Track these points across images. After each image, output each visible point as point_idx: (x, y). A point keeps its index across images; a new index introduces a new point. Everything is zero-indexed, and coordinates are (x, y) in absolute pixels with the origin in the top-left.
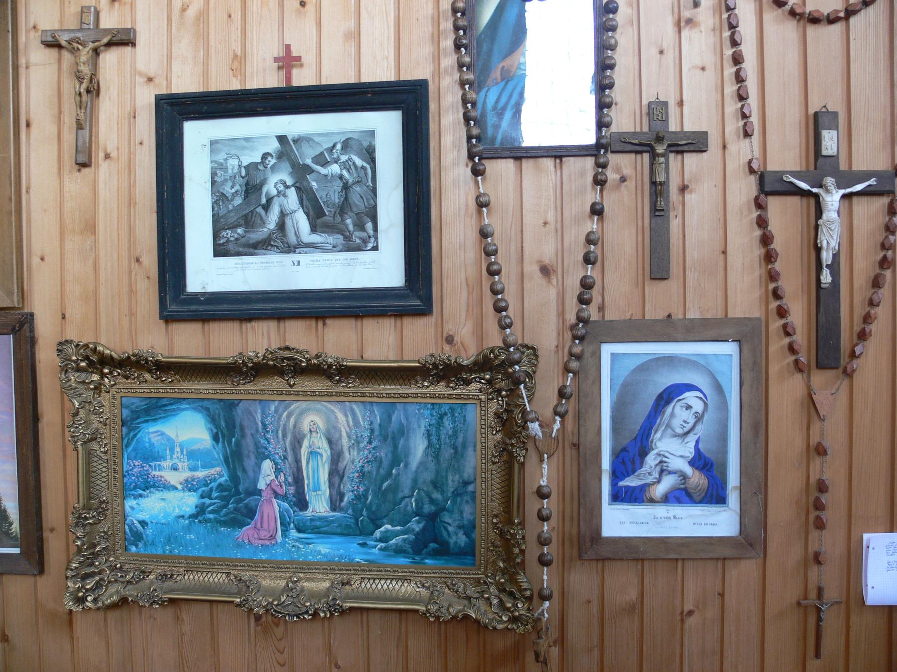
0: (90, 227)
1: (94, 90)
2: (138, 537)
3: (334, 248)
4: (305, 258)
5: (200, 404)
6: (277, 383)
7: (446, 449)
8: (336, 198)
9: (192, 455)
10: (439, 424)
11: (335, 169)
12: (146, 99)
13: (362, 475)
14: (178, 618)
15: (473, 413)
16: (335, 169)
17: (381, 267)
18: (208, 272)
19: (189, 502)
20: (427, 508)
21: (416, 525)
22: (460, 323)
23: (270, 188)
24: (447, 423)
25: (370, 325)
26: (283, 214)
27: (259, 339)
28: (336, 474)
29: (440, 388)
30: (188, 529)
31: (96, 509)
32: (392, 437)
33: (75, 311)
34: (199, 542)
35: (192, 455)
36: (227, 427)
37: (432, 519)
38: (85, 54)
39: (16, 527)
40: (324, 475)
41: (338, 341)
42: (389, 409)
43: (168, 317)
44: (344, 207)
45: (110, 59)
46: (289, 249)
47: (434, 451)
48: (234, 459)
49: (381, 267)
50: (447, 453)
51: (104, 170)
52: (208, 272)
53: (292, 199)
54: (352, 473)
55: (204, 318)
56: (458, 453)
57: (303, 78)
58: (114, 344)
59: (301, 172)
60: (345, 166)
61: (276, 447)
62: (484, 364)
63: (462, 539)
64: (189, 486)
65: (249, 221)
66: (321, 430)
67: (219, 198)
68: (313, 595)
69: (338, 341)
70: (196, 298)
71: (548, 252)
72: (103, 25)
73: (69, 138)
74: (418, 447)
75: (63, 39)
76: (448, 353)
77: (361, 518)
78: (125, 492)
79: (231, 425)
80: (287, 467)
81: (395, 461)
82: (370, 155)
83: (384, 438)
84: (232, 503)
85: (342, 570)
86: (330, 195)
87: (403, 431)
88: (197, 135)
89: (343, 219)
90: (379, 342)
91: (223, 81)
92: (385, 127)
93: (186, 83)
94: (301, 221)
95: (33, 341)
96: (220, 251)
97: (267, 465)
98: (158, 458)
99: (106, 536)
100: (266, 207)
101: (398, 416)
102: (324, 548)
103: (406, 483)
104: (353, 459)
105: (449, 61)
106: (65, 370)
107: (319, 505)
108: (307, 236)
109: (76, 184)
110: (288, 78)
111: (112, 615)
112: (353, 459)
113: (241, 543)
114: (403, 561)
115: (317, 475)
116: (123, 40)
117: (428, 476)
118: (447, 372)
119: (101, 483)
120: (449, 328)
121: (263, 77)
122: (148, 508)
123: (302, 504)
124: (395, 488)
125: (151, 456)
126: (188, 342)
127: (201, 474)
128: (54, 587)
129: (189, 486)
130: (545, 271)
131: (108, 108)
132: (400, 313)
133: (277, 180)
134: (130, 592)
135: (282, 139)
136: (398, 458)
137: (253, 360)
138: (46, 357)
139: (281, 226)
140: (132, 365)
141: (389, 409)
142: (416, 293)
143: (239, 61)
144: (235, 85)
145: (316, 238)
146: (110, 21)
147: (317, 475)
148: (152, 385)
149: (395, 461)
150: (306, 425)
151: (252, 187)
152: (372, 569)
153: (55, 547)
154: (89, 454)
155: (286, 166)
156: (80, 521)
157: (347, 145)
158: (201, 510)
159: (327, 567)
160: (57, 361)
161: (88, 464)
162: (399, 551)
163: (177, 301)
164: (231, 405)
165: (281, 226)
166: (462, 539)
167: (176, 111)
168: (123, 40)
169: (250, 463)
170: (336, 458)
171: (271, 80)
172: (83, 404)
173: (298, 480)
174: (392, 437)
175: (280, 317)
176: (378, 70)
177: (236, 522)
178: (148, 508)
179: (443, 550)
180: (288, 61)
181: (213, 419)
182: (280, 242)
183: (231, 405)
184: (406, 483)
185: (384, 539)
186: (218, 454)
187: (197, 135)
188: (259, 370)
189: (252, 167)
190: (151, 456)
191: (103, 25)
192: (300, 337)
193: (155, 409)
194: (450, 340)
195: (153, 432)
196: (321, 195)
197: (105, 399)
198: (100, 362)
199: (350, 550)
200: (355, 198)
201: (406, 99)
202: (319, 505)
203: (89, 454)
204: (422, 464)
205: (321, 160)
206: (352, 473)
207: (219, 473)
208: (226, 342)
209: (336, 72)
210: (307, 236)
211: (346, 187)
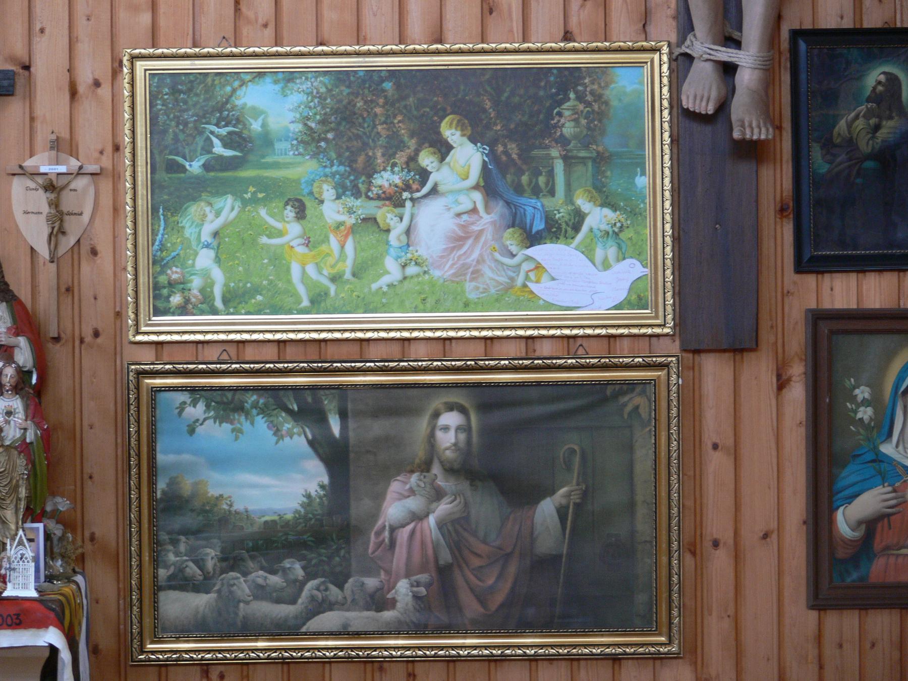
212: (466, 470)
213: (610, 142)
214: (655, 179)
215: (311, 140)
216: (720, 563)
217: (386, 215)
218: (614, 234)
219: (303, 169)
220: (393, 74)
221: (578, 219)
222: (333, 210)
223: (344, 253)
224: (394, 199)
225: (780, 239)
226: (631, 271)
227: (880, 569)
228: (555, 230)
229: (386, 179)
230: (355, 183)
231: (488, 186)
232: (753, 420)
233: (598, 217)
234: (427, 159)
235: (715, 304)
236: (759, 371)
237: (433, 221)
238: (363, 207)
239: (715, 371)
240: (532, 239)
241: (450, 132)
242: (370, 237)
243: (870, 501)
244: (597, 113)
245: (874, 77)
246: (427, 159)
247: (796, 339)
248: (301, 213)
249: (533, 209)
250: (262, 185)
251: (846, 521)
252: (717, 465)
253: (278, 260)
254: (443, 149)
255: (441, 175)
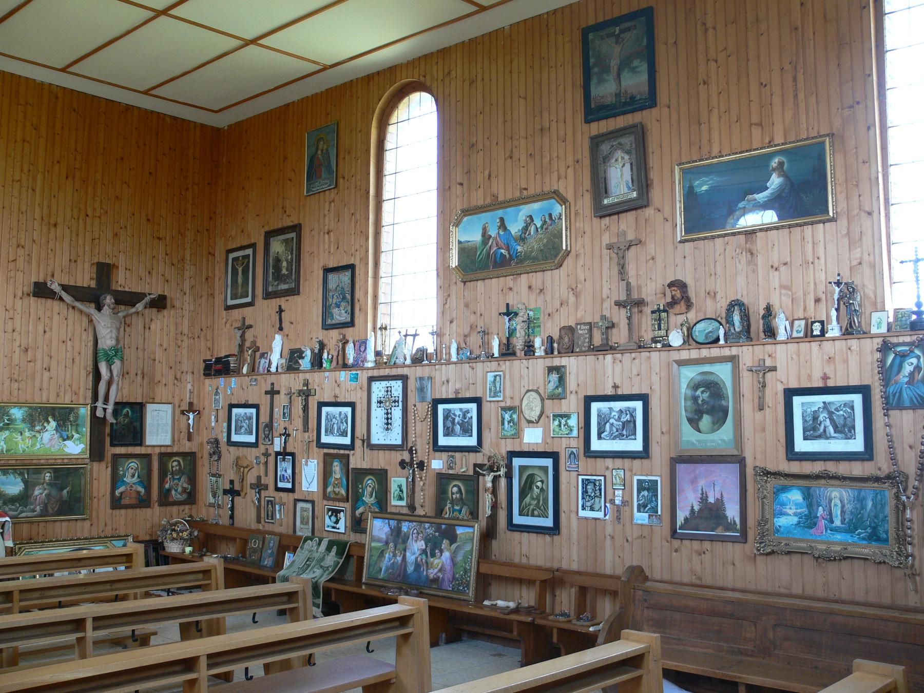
0: (763, 430)
1: (764, 386)
2: (778, 531)
3: (842, 438)
4: (832, 441)
5: (798, 487)
6: (823, 481)
7: (879, 505)
8: (842, 422)
9: (796, 504)
10: (876, 497)
11: (841, 412)
12: (780, 388)
13: (852, 513)
14: (791, 560)
15: (887, 493)
16: (841, 412)
17: (857, 445)
18: (801, 445)
19: (795, 520)
20: (873, 525)
21: (869, 530)
22: (881, 464)
23: (821, 418)
24: (879, 497)
25: (853, 464)
26: (825, 427)
27: (817, 467)
28: (843, 512)
29: (876, 485)
30: (795, 529)
31: (763, 521)
32: (861, 500)
33: (759, 457)
34: (798, 533)
35: (796, 504)
36: (808, 495)
37: (874, 529)
38: (761, 375)
39: (738, 527)
40: (839, 513)
41: (843, 468)
42: (860, 491)
43: (789, 459)
44: (844, 425)
45: (769, 375)
46: (827, 438)
47: (875, 505)
48: (810, 506)
49: (857, 445)
50: (879, 506)
51: (767, 410)
52: (801, 445)
53: (828, 422)
54: (848, 512)
55: (801, 460)
56: (883, 506)
57: (831, 383)
58: (771, 467)
59: (831, 414)
60: (845, 412)
61: (823, 503)
62: (888, 477)
63: (885, 536)
64: (795, 514)
65: (814, 429)
66: (838, 498)
67: (805, 421)
68: (835, 552)
69: (843, 468)
70: (797, 453)
71: (911, 440)
72: (767, 365)
73: (756, 401)
74: (870, 504)
75: (754, 369)
76: (879, 473)
77: (851, 527)
78: (774, 516)
79: (809, 494)
80: (827, 509)
81: (862, 508)
82: (852, 408)
83: (858, 500)
84: (809, 521)
85: (845, 545)
86: (840, 422)
87: (864, 499)
88: (797, 401)
89: (845, 430)
90: (857, 469)
91: (806, 384)
92: (857, 399)
93: (794, 385)
94: (831, 429)
95: (745, 466)
96: (805, 438)
97: (820, 508)
98: (785, 505)
99: (768, 530)
100: (820, 425)
101: (863, 493)
102: (839, 537)
103: (866, 515)
104: (849, 507)
105: (877, 377)
106: (756, 475)
107: (838, 522)
108: (833, 434)
109: (759, 415)
110: (826, 383)
111: (769, 557)
112: (849, 507)
113: (811, 534)
114: (865, 542)
115: (837, 512)
116: (774, 369)
117: (873, 514)
118: (877, 479)
119: (766, 512)
120: (879, 465)
121: (817, 383)
122: (781, 522)
123: (832, 522)
124: (862, 517)
125: (783, 504)
126: (795, 467)
127: (799, 511)
128: (750, 547)
129: (795, 514)
130: (911, 447)
131: (768, 391)
132: (863, 460)
133: (823, 416)
134: (775, 549)
135: (824, 403)
136: (863, 507)
137: (815, 474)
138: (749, 471)
139: (825, 431)
140: (777, 474)
141: (860, 491)
142: (868, 454)
143: (809, 377)
144: (809, 386)
145: (836, 435)
146: (768, 363)
147: (837, 512)
148: (783, 481)
149: (862, 508)
150: (833, 496)
151: (815, 418)
152: (854, 544)
153: (751, 535)
154: (763, 503)
155: (826, 411)
156: (759, 524)
157: (845, 405)
158: (799, 523)
159: (840, 543)
160: (753, 472)
161: (763, 506)
162: (863, 539)
163: (791, 454)
164: (809, 488)
165: (825, 431)
166: (885, 536)
167: (790, 393)
168: (774, 369)
169: (815, 507)
170: (843, 507)
171: (820, 384)
172: (762, 486)
173: (831, 514)
174: (861, 500)
175: (825, 460)
176: (854, 382)
177: (810, 527)
178: (781, 522)
179: (878, 539)
180: (825, 378)
181: (803, 493)
182: (824, 436)
183: (809, 488)
184: (866, 515)
185: (859, 534)
186: (805, 505)
187: (797, 401)
188: (817, 477)
189: (815, 412)
190: (783, 504)
191: (767, 365)
192: (831, 467)
193: (785, 489)
194: (880, 469)
195: (784, 496)
196: (837, 421)
197: (768, 485)
198: (767, 473)
199: (847, 538)
200: (848, 422)
201: (864, 391)
202: (838, 522)
203: (763, 503)
204: (871, 510)
205: (837, 410)
206: (848, 512)
207: (805, 510)
208: (808, 468)
209: (841, 383)
210: (833, 434)
211: (845, 418)
212: (50, 484)
213: (79, 422)
214: (86, 429)
215: (24, 420)
216: (95, 501)
217: (37, 435)
218: (79, 439)
219: (22, 426)
220: (40, 407)
221: (73, 436)
222: (27, 434)
223: (29, 442)
224: (39, 432)
225: (108, 440)
226: (82, 446)
227: (124, 502)
228: (69, 438)
229: (38, 428)
230: (32, 428)
231: (56, 430)
232: (101, 473)
233: (76, 436)
234: (45, 424)
235: (96, 452)
236: (103, 465)
237: (46, 436)
238: (33, 433)
239: (95, 464)
240: (64, 440)
241: (50, 419)
242: (34, 439)
243: (122, 489)
244: (77, 417)
245: (125, 411)
246: (45, 424)
247: (110, 459)
248: (21, 434)
249: (65, 434)
250: (15, 429)
251: (117, 493)
252: (95, 482)
253: (17, 443)
254: (48, 422)
255: (48, 427)
